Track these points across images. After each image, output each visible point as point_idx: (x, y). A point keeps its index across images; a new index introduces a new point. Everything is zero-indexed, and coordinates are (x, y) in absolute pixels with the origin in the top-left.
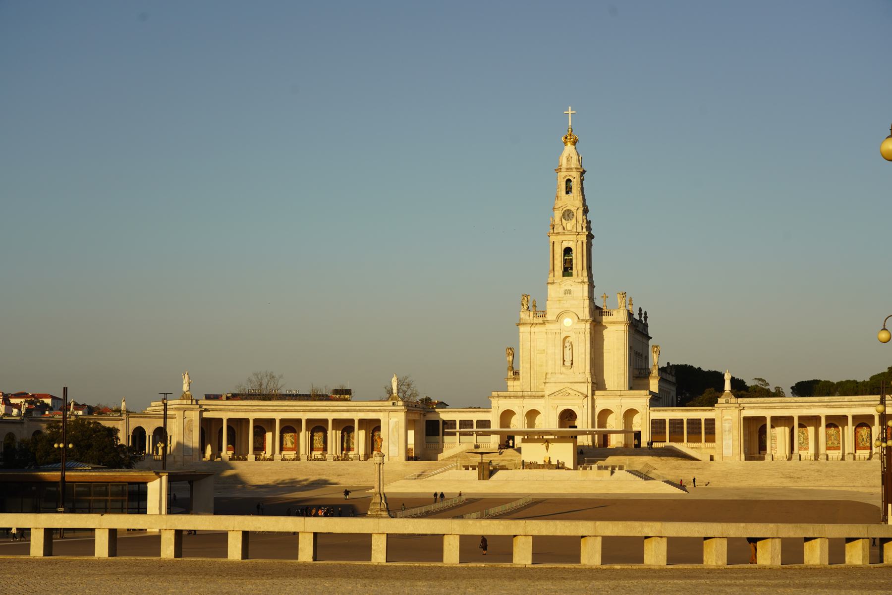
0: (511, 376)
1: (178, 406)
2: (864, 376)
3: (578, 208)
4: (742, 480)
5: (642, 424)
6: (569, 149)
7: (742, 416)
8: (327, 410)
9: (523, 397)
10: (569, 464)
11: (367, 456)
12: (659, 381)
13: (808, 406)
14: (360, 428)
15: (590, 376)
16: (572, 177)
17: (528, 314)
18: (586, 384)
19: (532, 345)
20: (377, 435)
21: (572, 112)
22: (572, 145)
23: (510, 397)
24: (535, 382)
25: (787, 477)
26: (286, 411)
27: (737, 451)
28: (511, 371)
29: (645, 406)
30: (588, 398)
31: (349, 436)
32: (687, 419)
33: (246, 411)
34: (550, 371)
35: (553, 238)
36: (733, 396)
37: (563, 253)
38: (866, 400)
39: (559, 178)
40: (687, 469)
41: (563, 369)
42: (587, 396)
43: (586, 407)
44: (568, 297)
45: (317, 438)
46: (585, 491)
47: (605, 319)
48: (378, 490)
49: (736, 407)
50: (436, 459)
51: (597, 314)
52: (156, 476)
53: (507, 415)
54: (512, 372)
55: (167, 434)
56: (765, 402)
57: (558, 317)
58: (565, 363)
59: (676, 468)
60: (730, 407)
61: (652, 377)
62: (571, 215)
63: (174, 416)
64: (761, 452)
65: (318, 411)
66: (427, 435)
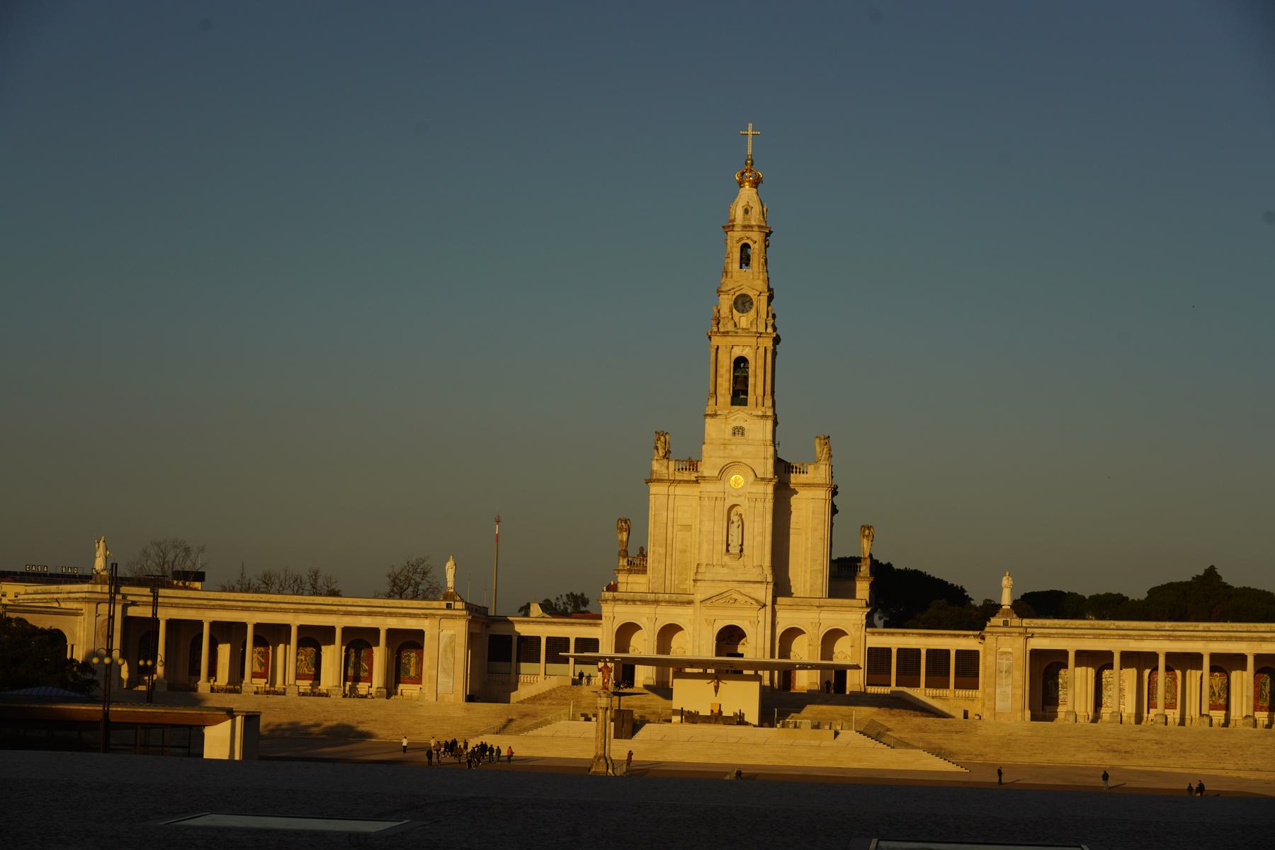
0: (624, 566)
1: (87, 595)
2: (1137, 592)
3: (761, 293)
4: (1035, 754)
5: (845, 653)
6: (747, 194)
7: (1029, 648)
8: (335, 611)
9: (656, 602)
10: (752, 715)
11: (390, 690)
12: (870, 585)
13: (1138, 636)
14: (1078, 664)
15: (770, 572)
16: (752, 241)
17: (666, 464)
18: (764, 586)
19: (671, 516)
20: (406, 656)
21: (754, 133)
22: (751, 187)
23: (634, 601)
24: (673, 578)
25: (1108, 751)
26: (266, 610)
27: (1019, 705)
28: (624, 557)
29: (858, 625)
30: (767, 607)
31: (358, 657)
32: (927, 650)
33: (199, 607)
34: (704, 562)
35: (716, 340)
36: (1015, 616)
37: (732, 365)
38: (1235, 629)
39: (729, 241)
40: (940, 731)
41: (726, 559)
42: (765, 605)
43: (762, 623)
44: (738, 438)
45: (303, 658)
46: (799, 763)
47: (795, 479)
48: (603, 753)
49: (1020, 634)
50: (507, 701)
51: (783, 469)
52: (227, 717)
53: (626, 631)
54: (626, 560)
55: (66, 641)
56: (1067, 626)
57: (722, 471)
58: (730, 548)
59: (920, 729)
60: (1011, 633)
61: (861, 578)
62: (747, 305)
63: (80, 611)
64: (1045, 707)
65: (319, 612)
66: (489, 660)
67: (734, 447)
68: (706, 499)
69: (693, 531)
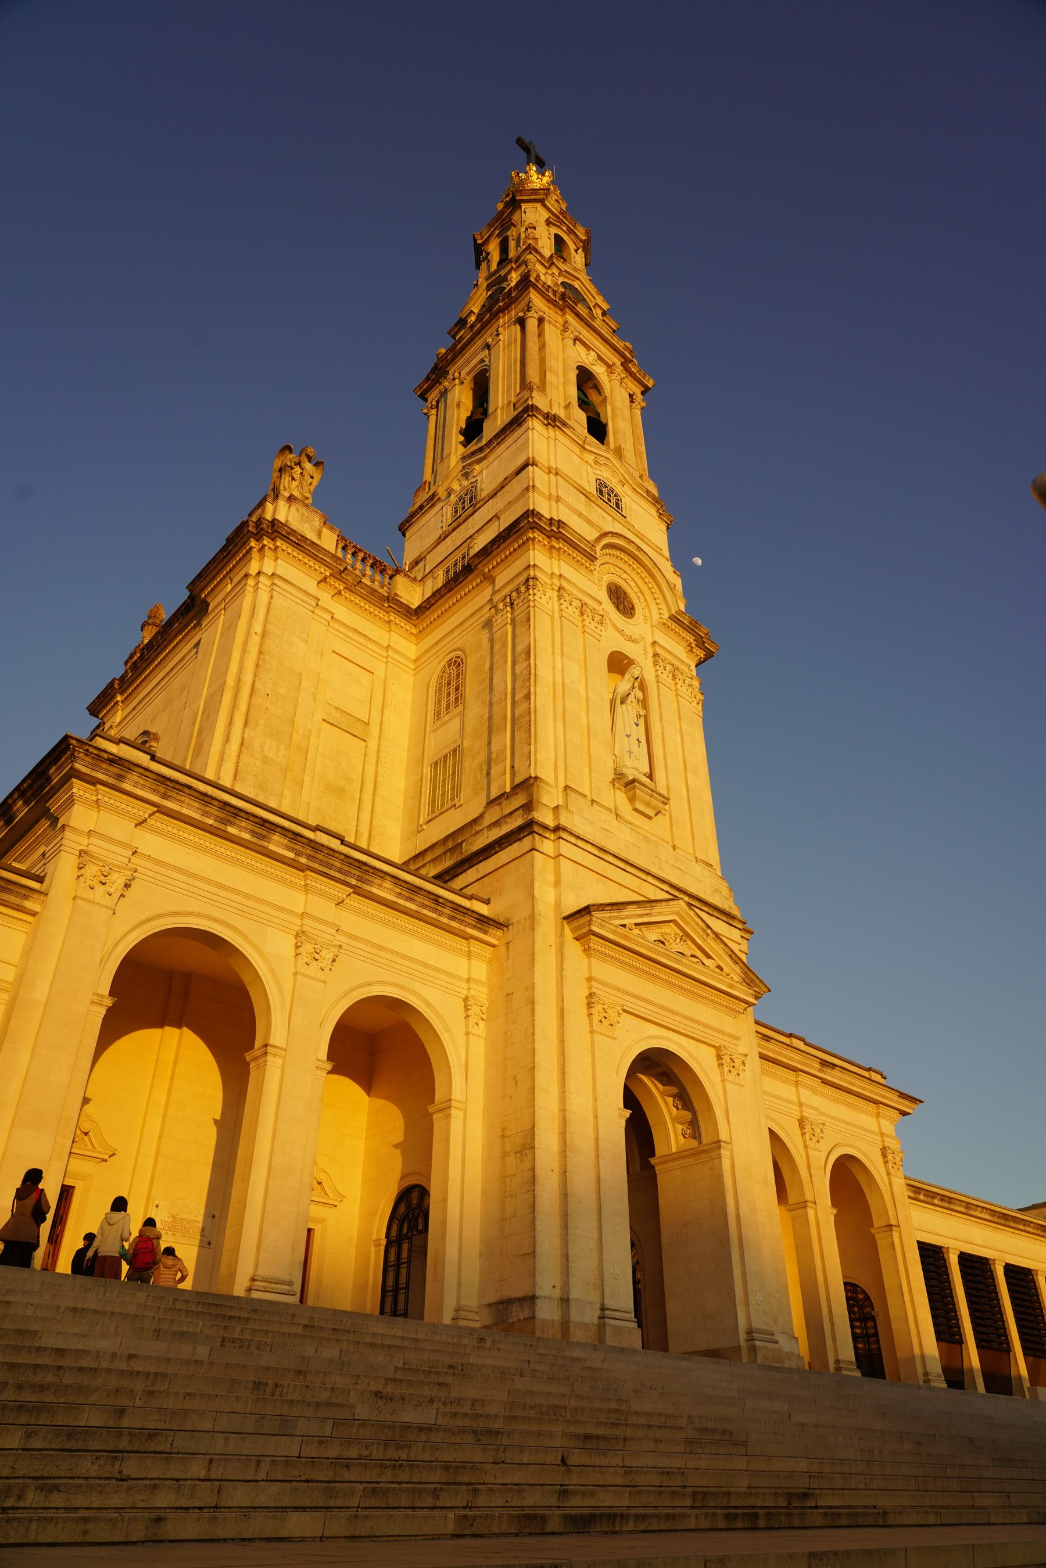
67: (609, 519)
69: (373, 743)
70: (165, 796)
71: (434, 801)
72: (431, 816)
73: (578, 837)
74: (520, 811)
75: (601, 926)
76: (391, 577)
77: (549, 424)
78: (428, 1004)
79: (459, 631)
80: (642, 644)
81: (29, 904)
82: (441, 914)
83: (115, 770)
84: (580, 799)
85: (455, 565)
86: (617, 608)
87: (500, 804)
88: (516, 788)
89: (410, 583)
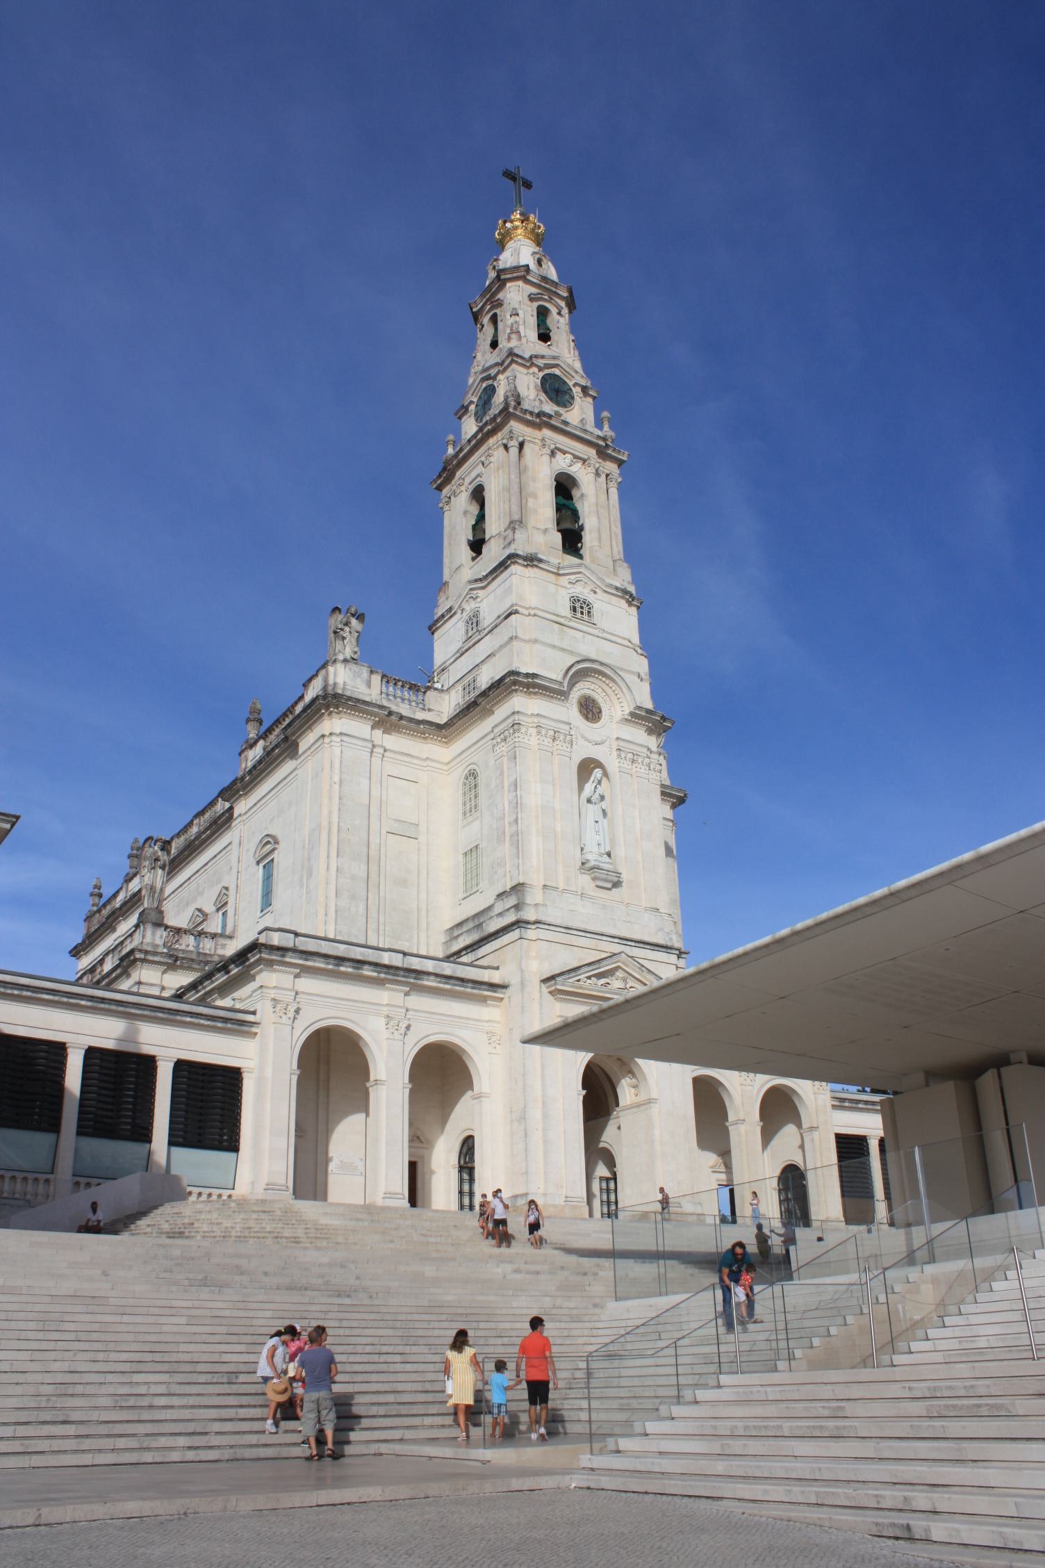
19: (376, 793)
68: (533, 731)
69: (422, 838)
70: (306, 960)
71: (466, 882)
72: (465, 895)
73: (549, 925)
74: (513, 909)
75: (562, 985)
76: (425, 693)
77: (528, 565)
78: (462, 1039)
79: (473, 749)
80: (607, 742)
81: (254, 1030)
82: (466, 987)
83: (280, 953)
84: (554, 893)
85: (469, 685)
86: (587, 718)
87: (502, 900)
88: (513, 888)
89: (439, 694)
